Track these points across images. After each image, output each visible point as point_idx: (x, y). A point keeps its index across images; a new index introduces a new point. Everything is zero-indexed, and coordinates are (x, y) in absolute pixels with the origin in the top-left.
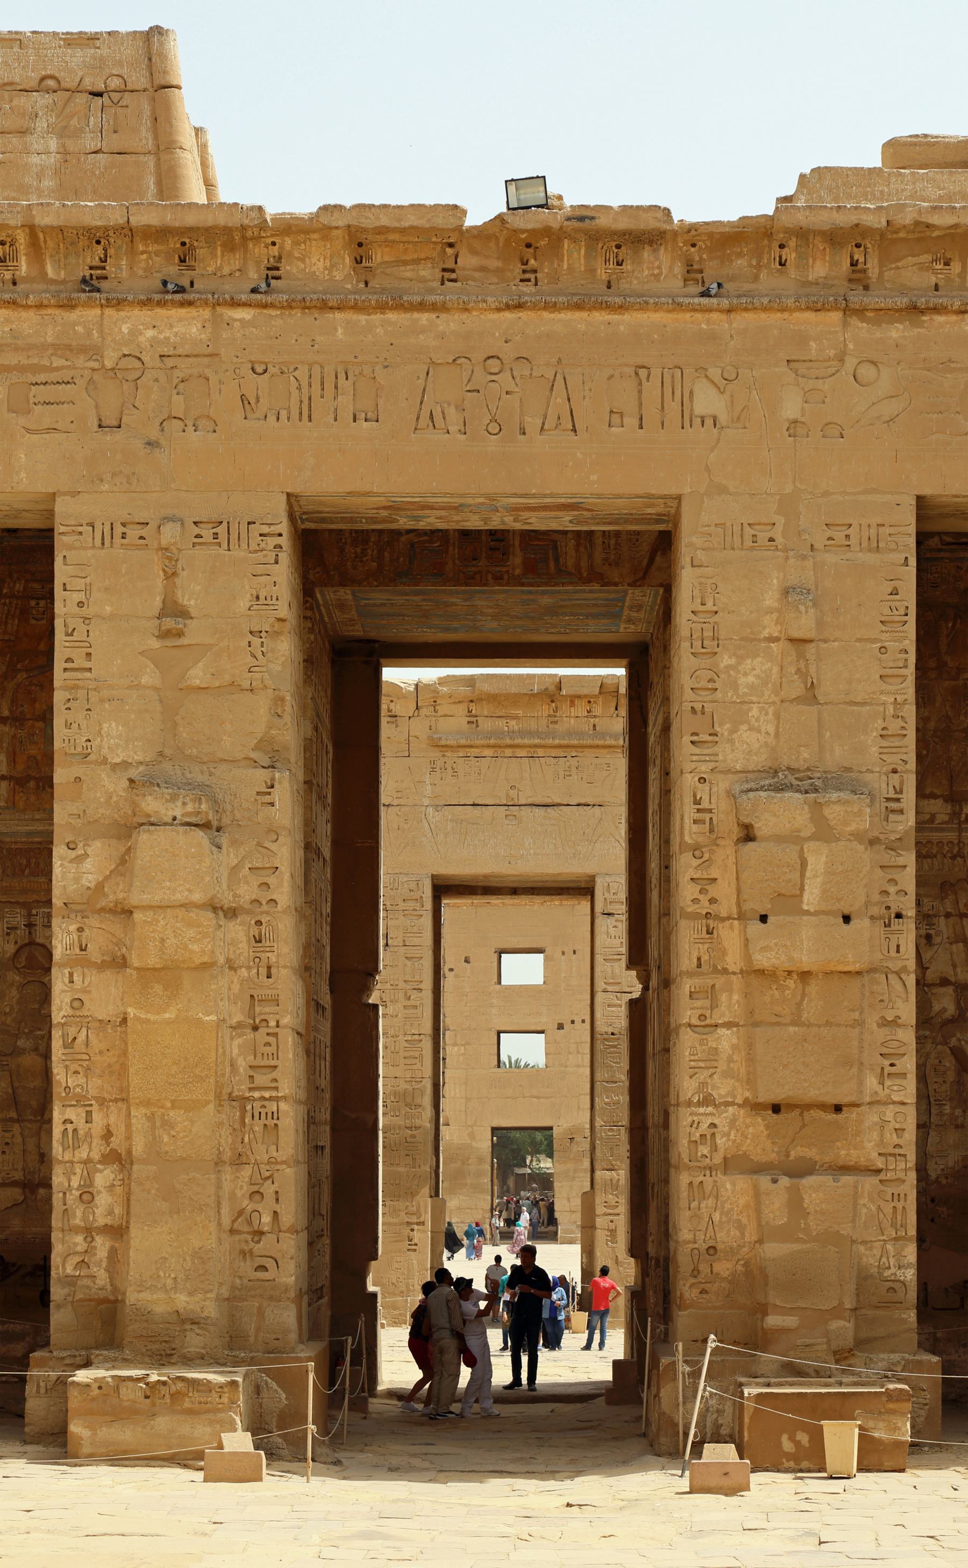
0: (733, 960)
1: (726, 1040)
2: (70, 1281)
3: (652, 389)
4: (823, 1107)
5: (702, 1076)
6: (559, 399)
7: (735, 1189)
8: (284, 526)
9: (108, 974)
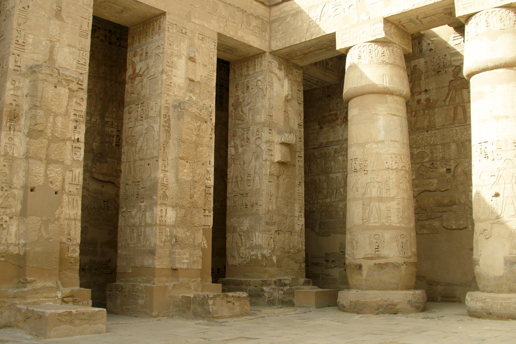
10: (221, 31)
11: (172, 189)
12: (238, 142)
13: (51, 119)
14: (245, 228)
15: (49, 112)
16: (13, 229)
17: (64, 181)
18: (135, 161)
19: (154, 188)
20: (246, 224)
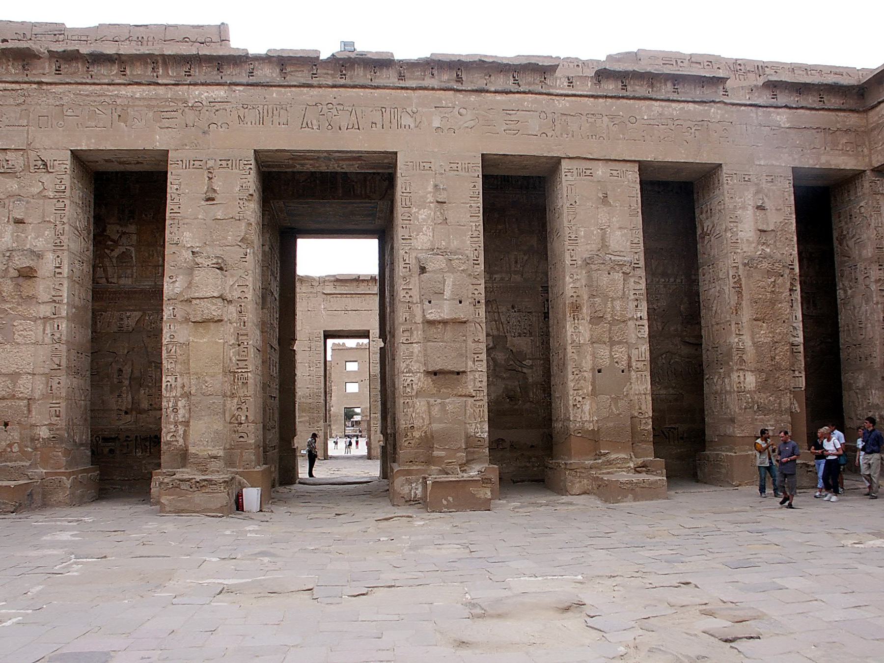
0: (419, 319)
1: (416, 348)
2: (168, 443)
3: (387, 115)
4: (452, 372)
5: (408, 362)
6: (353, 118)
7: (420, 405)
8: (253, 162)
9: (184, 326)
10: (797, 164)
11: (750, 354)
12: (846, 283)
13: (609, 305)
14: (860, 385)
15: (606, 297)
16: (587, 408)
17: (630, 358)
18: (712, 326)
19: (729, 354)
20: (861, 380)
